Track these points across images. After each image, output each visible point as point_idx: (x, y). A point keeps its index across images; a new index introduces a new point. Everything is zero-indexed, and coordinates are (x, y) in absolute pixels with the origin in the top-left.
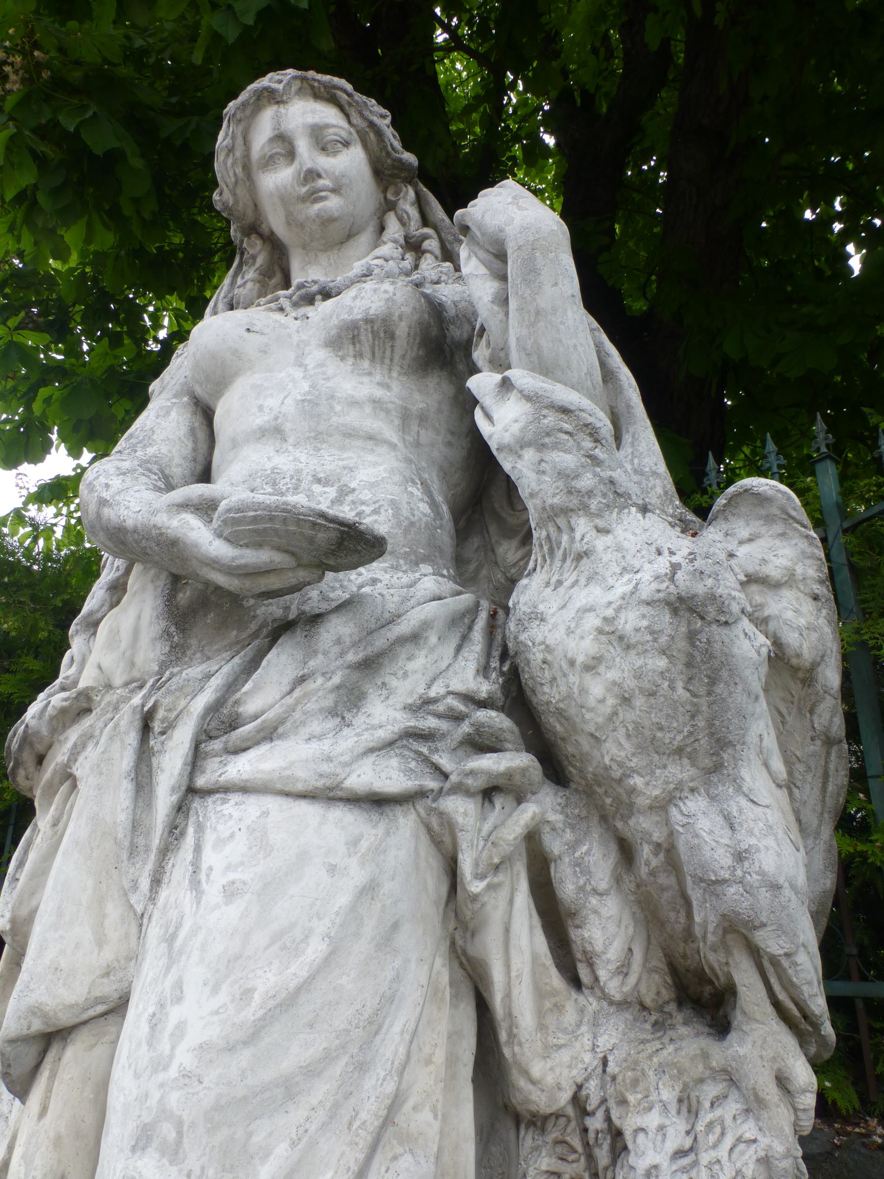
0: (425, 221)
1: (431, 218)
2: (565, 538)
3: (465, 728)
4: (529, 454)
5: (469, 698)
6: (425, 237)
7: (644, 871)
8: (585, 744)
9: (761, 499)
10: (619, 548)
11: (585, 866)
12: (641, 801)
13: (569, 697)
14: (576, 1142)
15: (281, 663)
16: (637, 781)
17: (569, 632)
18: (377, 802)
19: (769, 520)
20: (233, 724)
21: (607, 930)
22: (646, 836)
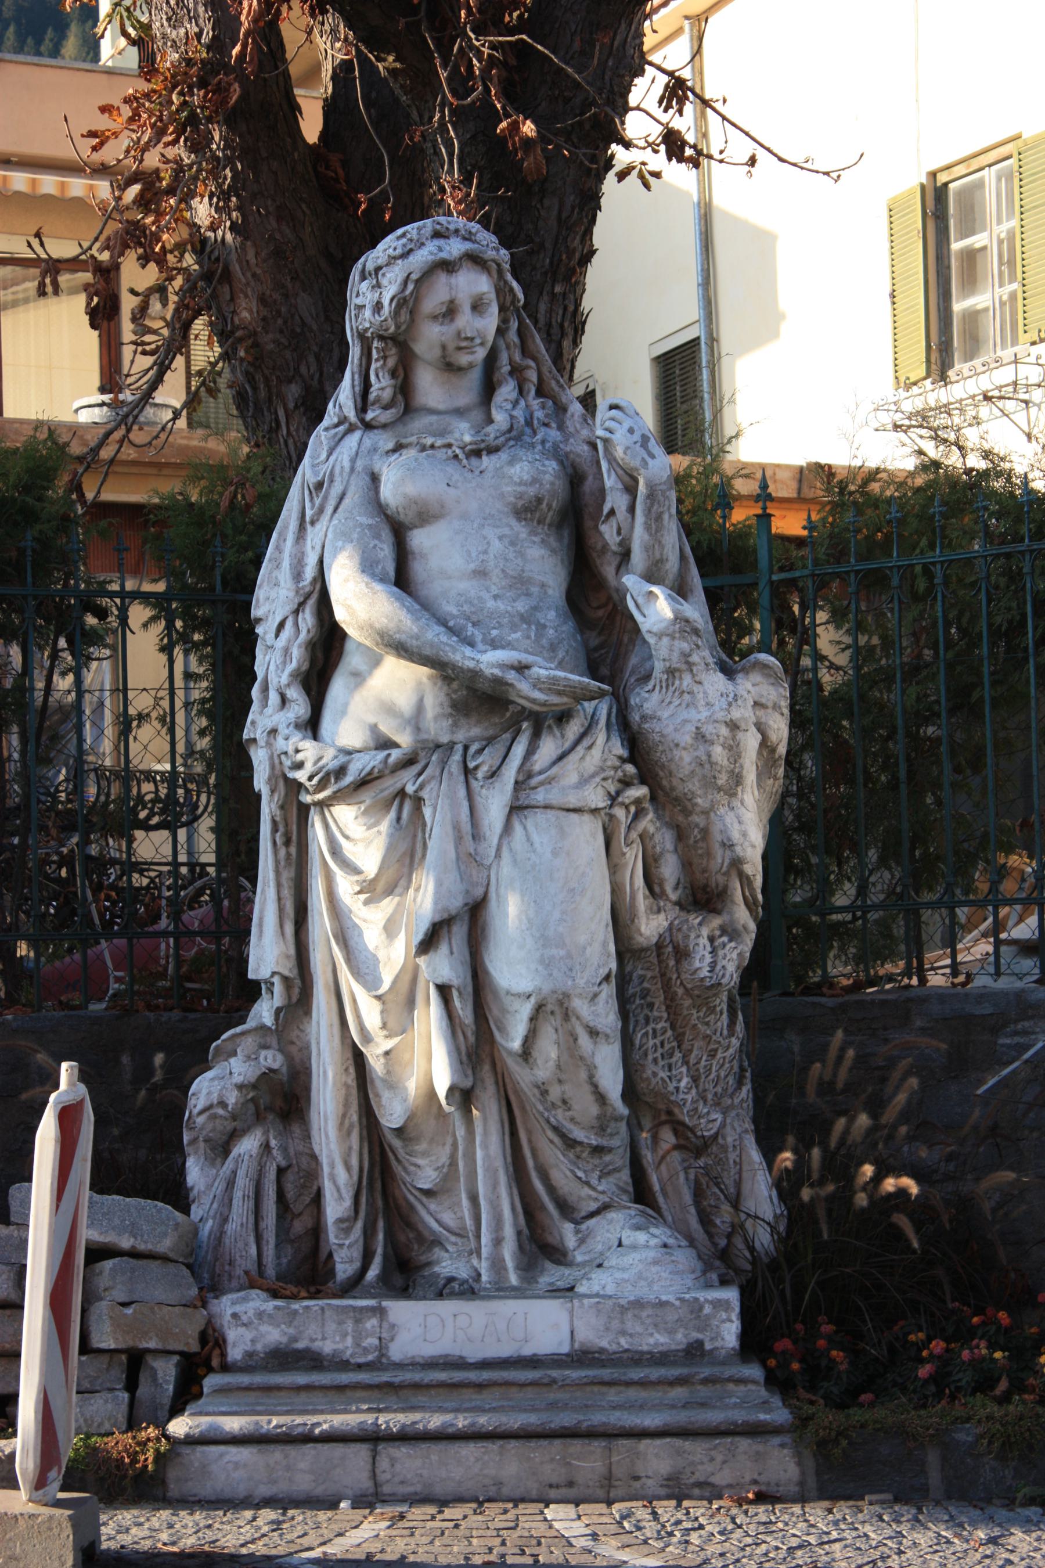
0: (525, 352)
1: (532, 347)
2: (677, 682)
3: (620, 773)
4: (665, 640)
5: (620, 758)
6: (528, 367)
7: (691, 841)
8: (675, 782)
9: (765, 666)
10: (705, 693)
11: (664, 840)
12: (698, 809)
13: (671, 760)
14: (655, 961)
15: (548, 748)
16: (699, 801)
17: (676, 730)
18: (595, 811)
19: (768, 676)
20: (530, 776)
21: (669, 870)
22: (697, 825)
